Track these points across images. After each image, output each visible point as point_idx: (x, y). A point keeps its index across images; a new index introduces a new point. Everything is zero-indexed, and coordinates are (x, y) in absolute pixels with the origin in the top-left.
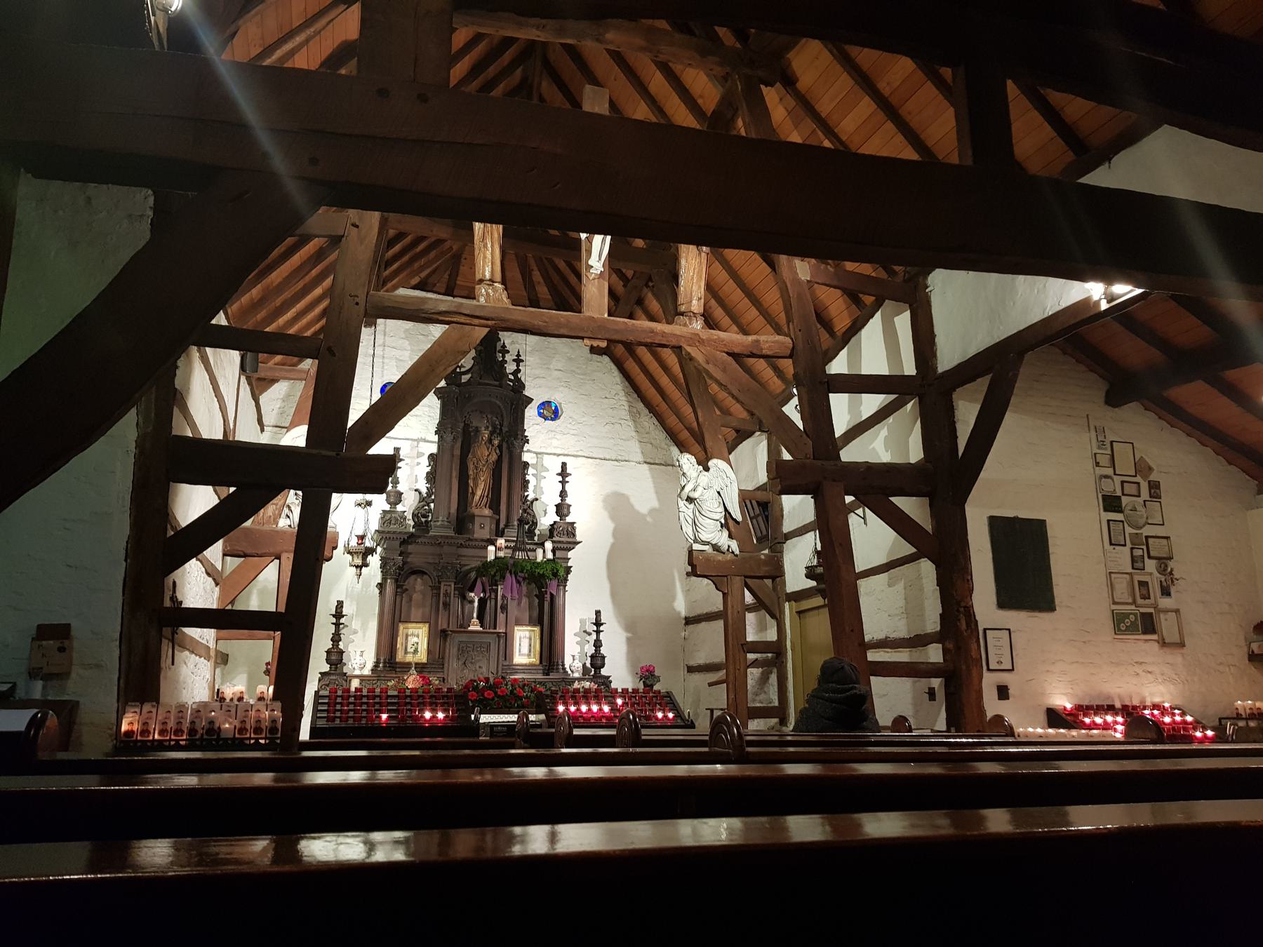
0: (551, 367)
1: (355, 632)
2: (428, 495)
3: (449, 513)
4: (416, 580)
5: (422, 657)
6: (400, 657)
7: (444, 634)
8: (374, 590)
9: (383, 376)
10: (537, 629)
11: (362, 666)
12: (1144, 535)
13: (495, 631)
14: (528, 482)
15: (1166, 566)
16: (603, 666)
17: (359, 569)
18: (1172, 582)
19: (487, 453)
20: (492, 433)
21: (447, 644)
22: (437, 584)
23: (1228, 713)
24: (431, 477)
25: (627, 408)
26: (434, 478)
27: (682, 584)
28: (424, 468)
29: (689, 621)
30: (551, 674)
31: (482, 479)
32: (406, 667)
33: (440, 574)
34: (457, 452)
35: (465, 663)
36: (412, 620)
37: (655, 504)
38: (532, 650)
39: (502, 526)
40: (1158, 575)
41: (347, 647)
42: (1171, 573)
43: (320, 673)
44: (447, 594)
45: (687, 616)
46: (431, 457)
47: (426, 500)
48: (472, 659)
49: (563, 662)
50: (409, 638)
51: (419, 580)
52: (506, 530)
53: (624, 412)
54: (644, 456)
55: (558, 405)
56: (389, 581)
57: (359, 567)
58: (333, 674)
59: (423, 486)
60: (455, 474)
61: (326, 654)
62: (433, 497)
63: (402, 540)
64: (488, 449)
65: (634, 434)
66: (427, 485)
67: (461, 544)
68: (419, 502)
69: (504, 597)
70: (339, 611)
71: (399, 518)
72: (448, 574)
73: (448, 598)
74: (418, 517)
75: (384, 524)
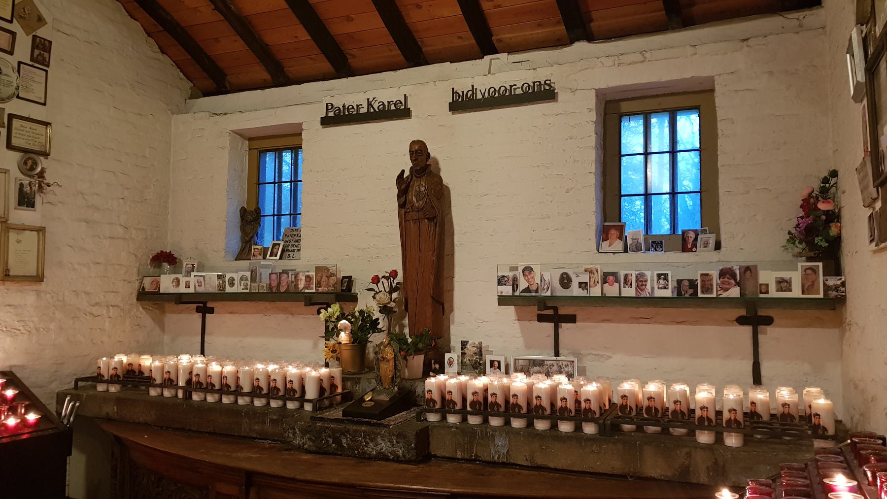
12: (7, 112)
15: (35, 164)
18: (40, 187)
23: (91, 372)
40: (21, 176)
42: (41, 175)
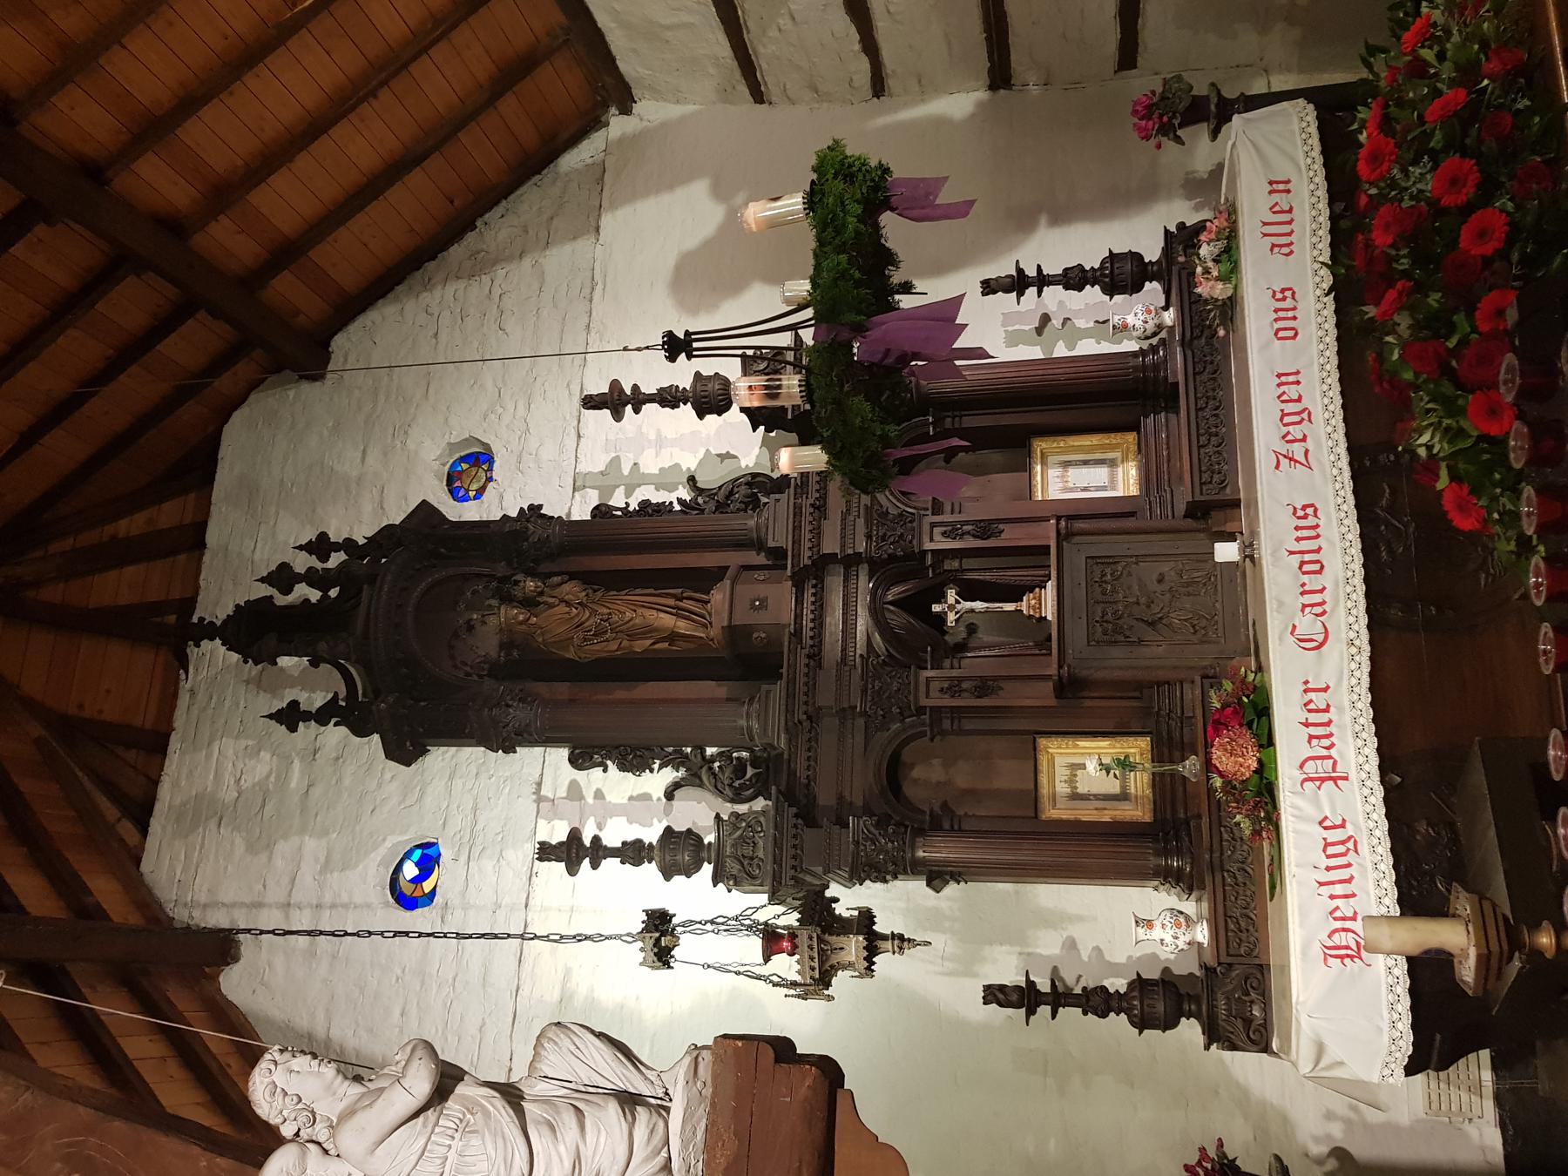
0: (355, 473)
1: (1071, 945)
2: (682, 764)
3: (728, 700)
4: (915, 781)
5: (1137, 748)
6: (1138, 812)
7: (1070, 687)
8: (948, 899)
9: (369, 906)
10: (1039, 445)
11: (1182, 920)
13: (1053, 551)
14: (645, 504)
16: (1136, 257)
17: (882, 945)
19: (563, 608)
20: (507, 599)
21: (1100, 675)
22: (926, 717)
24: (634, 760)
25: (461, 284)
26: (633, 750)
27: (906, 105)
28: (613, 782)
29: (1000, 77)
30: (1170, 380)
31: (629, 615)
32: (1166, 788)
33: (895, 710)
34: (562, 690)
35: (1152, 624)
36: (1032, 786)
37: (699, 189)
38: (1098, 456)
39: (761, 559)
41: (1115, 969)
43: (1207, 1048)
44: (954, 688)
45: (985, 79)
46: (578, 761)
47: (695, 769)
48: (1138, 603)
49: (1134, 354)
50: (1082, 789)
51: (916, 773)
52: (771, 544)
53: (474, 291)
54: (584, 234)
55: (457, 456)
56: (920, 854)
57: (873, 943)
58: (1212, 1007)
59: (659, 779)
60: (621, 693)
61: (1146, 1032)
62: (689, 750)
63: (800, 821)
64: (551, 606)
65: (527, 262)
66: (656, 766)
67: (809, 657)
68: (701, 785)
69: (952, 532)
70: (1014, 997)
71: (739, 833)
72: (895, 687)
73: (965, 685)
74: (743, 787)
75: (753, 877)
